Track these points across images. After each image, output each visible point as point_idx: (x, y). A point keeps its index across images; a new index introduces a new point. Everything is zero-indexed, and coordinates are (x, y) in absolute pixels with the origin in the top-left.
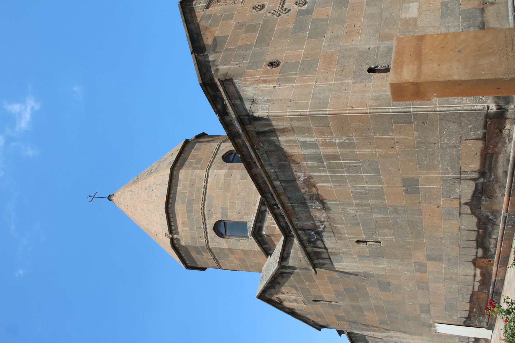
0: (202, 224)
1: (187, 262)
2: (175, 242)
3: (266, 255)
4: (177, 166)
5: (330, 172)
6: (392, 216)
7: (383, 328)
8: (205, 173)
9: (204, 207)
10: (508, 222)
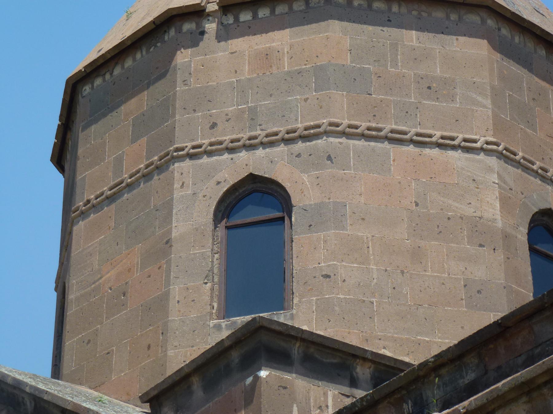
0: (269, 131)
1: (98, 82)
2: (188, 26)
3: (155, 393)
4: (499, 29)
8: (483, 139)
9: (343, 134)
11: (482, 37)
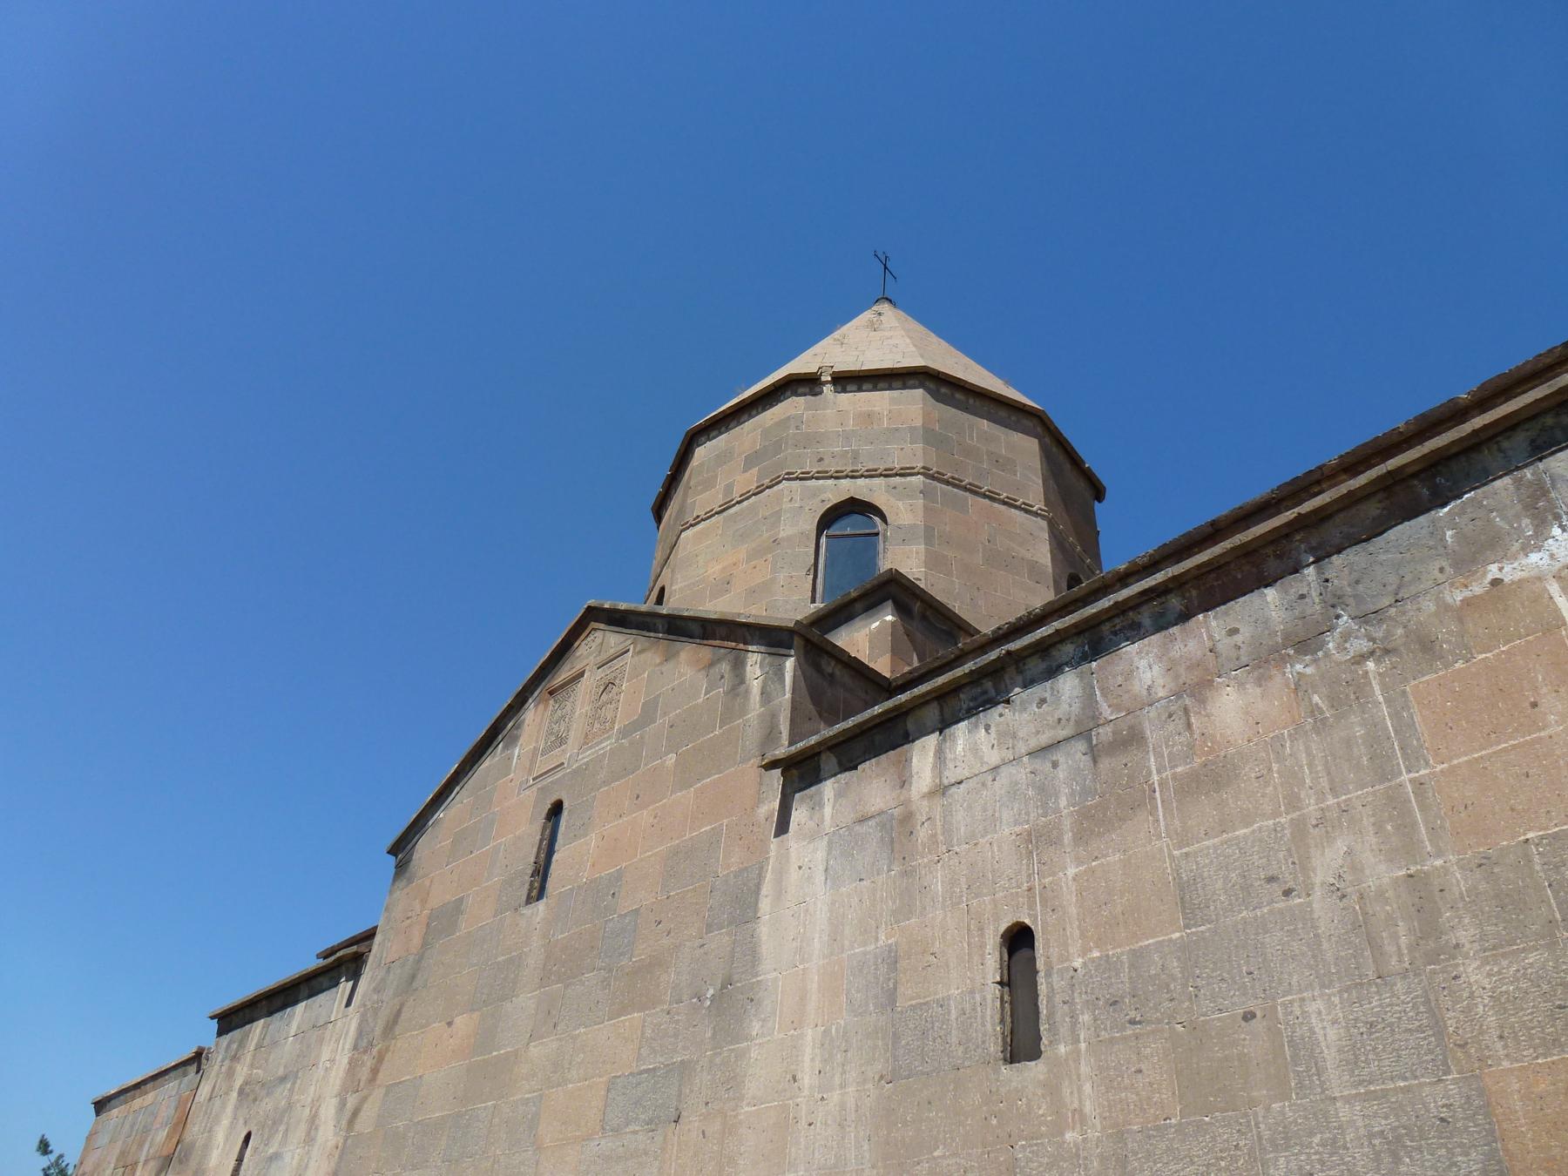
7: (364, 1100)
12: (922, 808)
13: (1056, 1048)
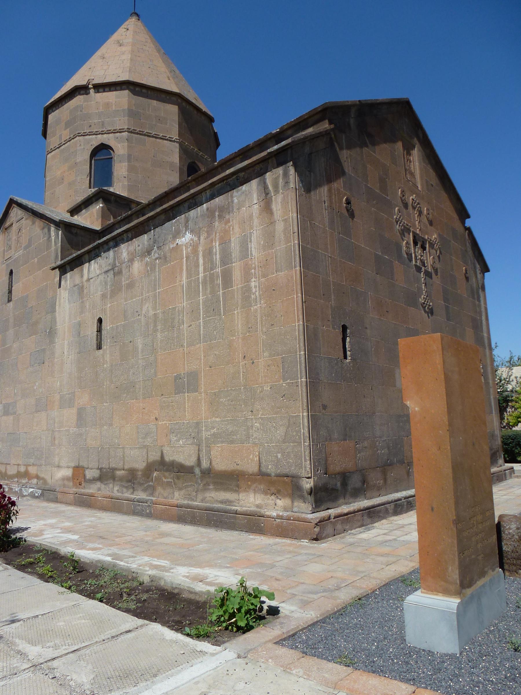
4: (182, 103)
5: (205, 277)
6: (140, 361)
10: (139, 505)
11: (176, 105)
12: (85, 284)
13: (104, 347)
